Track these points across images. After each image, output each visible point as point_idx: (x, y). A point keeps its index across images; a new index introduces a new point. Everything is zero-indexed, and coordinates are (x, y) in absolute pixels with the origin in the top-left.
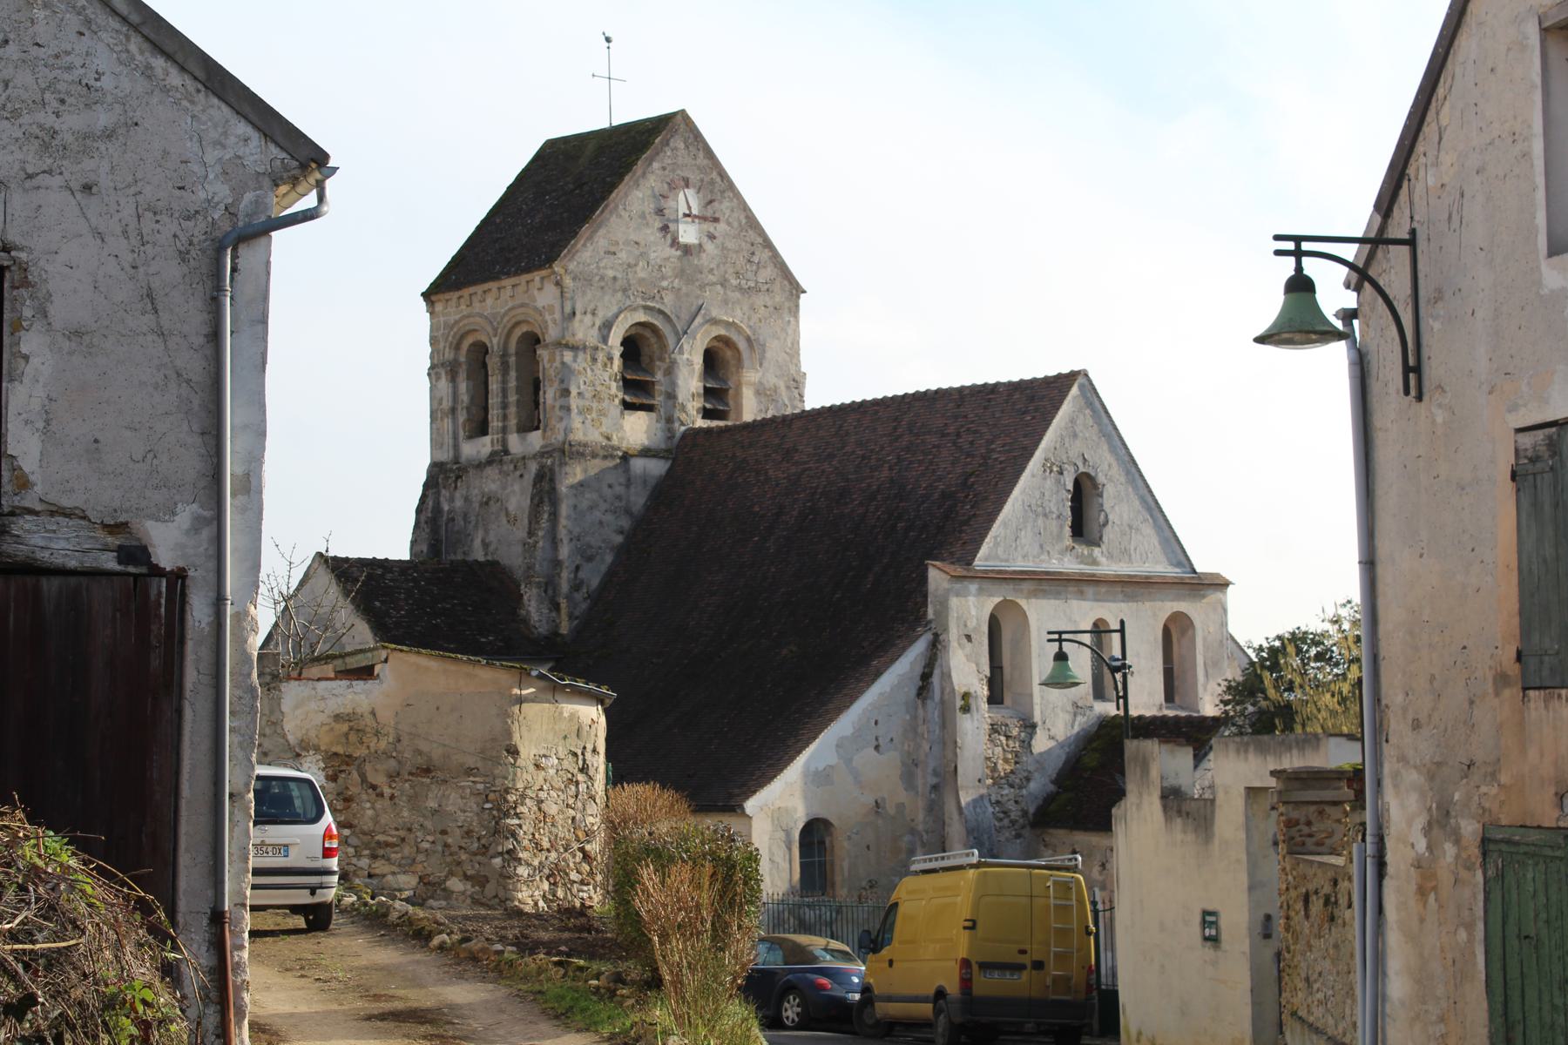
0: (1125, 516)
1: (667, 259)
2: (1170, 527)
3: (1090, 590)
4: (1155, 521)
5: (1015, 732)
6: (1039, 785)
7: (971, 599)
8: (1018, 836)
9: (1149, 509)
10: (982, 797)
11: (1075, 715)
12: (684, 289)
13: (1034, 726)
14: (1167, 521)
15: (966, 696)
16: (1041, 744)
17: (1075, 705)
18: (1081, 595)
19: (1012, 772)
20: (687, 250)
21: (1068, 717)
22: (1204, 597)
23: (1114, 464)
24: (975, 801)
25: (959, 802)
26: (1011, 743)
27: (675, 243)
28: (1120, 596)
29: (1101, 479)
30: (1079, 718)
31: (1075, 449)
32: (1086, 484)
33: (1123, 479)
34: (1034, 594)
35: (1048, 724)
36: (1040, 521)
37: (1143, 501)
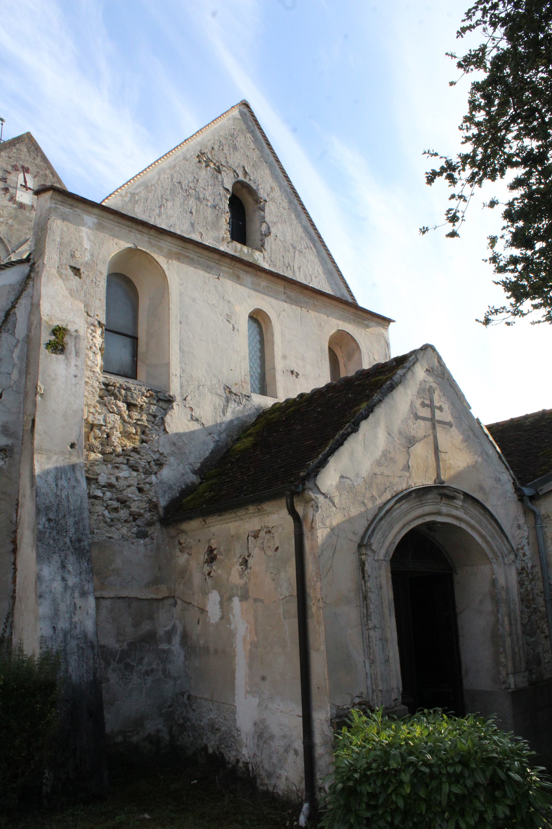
0: (289, 237)
1: (6, 207)
2: (334, 262)
3: (248, 279)
4: (318, 252)
5: (141, 401)
6: (175, 474)
7: (84, 229)
8: (141, 535)
9: (312, 239)
10: (73, 467)
11: (228, 401)
12: (16, 227)
13: (170, 401)
14: (329, 255)
15: (59, 332)
16: (178, 422)
17: (228, 389)
18: (237, 279)
19: (135, 450)
20: (21, 206)
21: (220, 402)
22: (368, 327)
23: (277, 189)
24: (60, 472)
25: (32, 469)
26: (135, 415)
27: (12, 199)
28: (283, 297)
29: (262, 194)
30: (232, 406)
31: (236, 160)
32: (248, 201)
33: (285, 204)
34: (179, 257)
35: (190, 402)
36: (192, 202)
37: (305, 229)
